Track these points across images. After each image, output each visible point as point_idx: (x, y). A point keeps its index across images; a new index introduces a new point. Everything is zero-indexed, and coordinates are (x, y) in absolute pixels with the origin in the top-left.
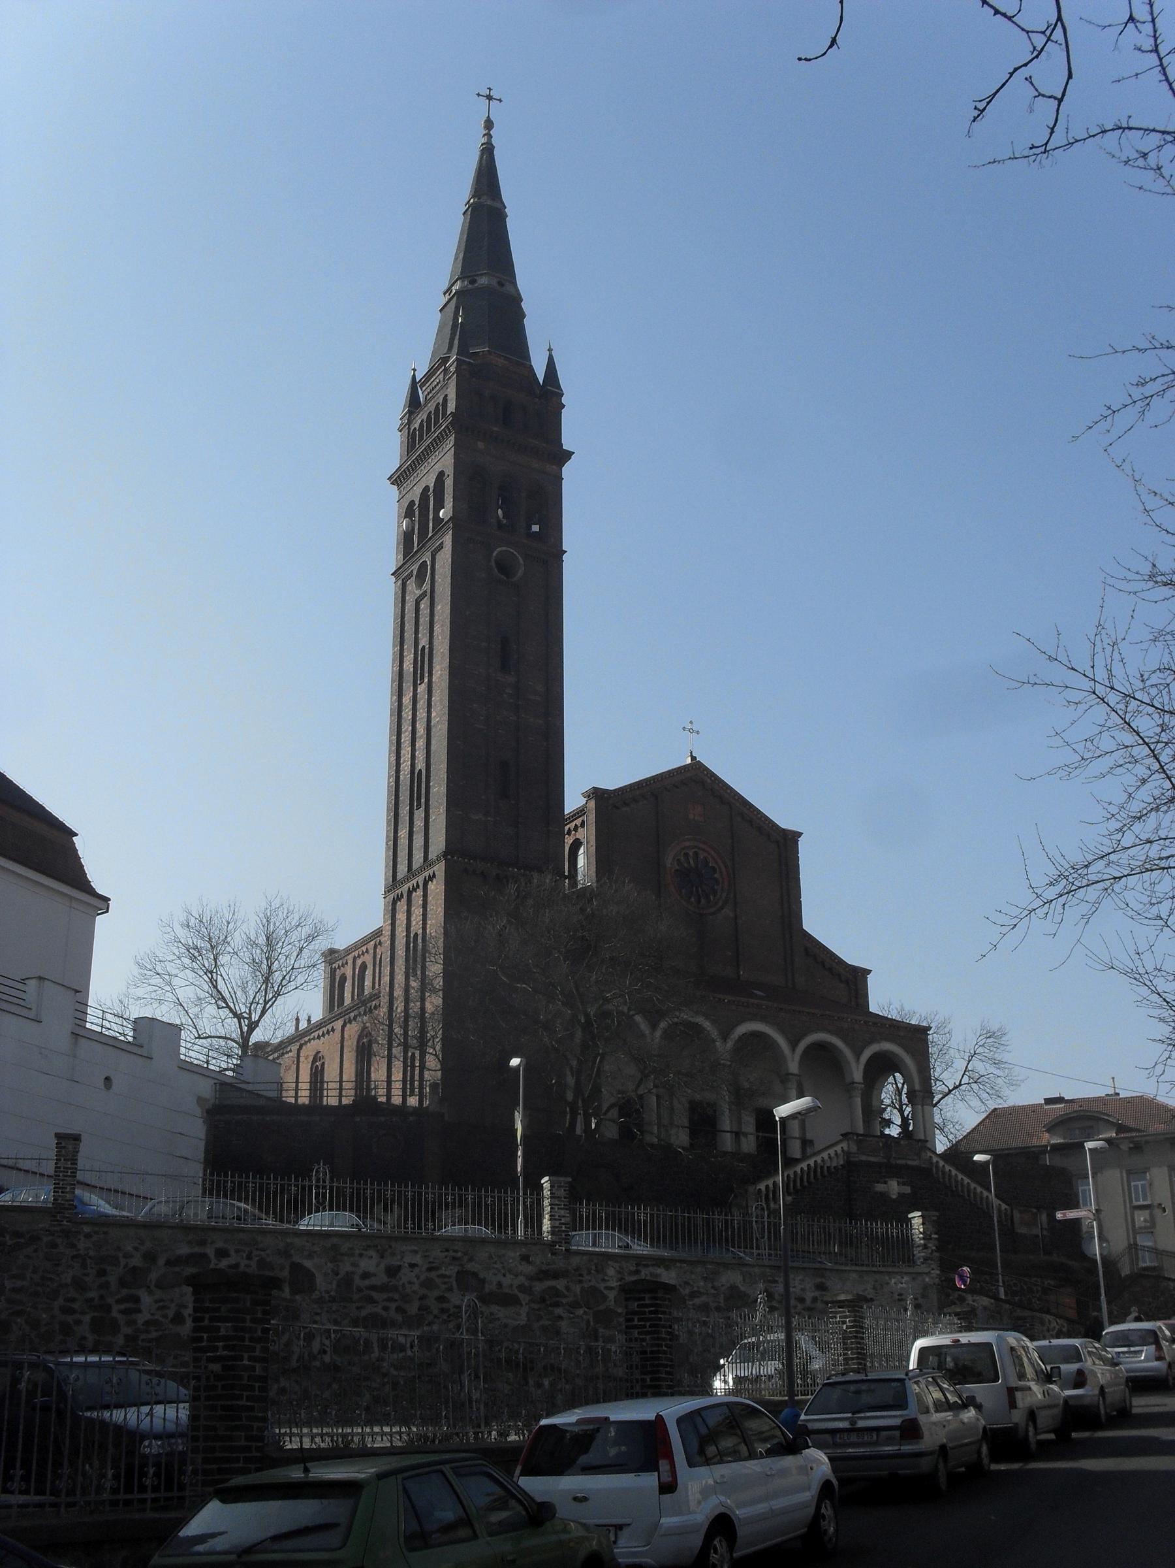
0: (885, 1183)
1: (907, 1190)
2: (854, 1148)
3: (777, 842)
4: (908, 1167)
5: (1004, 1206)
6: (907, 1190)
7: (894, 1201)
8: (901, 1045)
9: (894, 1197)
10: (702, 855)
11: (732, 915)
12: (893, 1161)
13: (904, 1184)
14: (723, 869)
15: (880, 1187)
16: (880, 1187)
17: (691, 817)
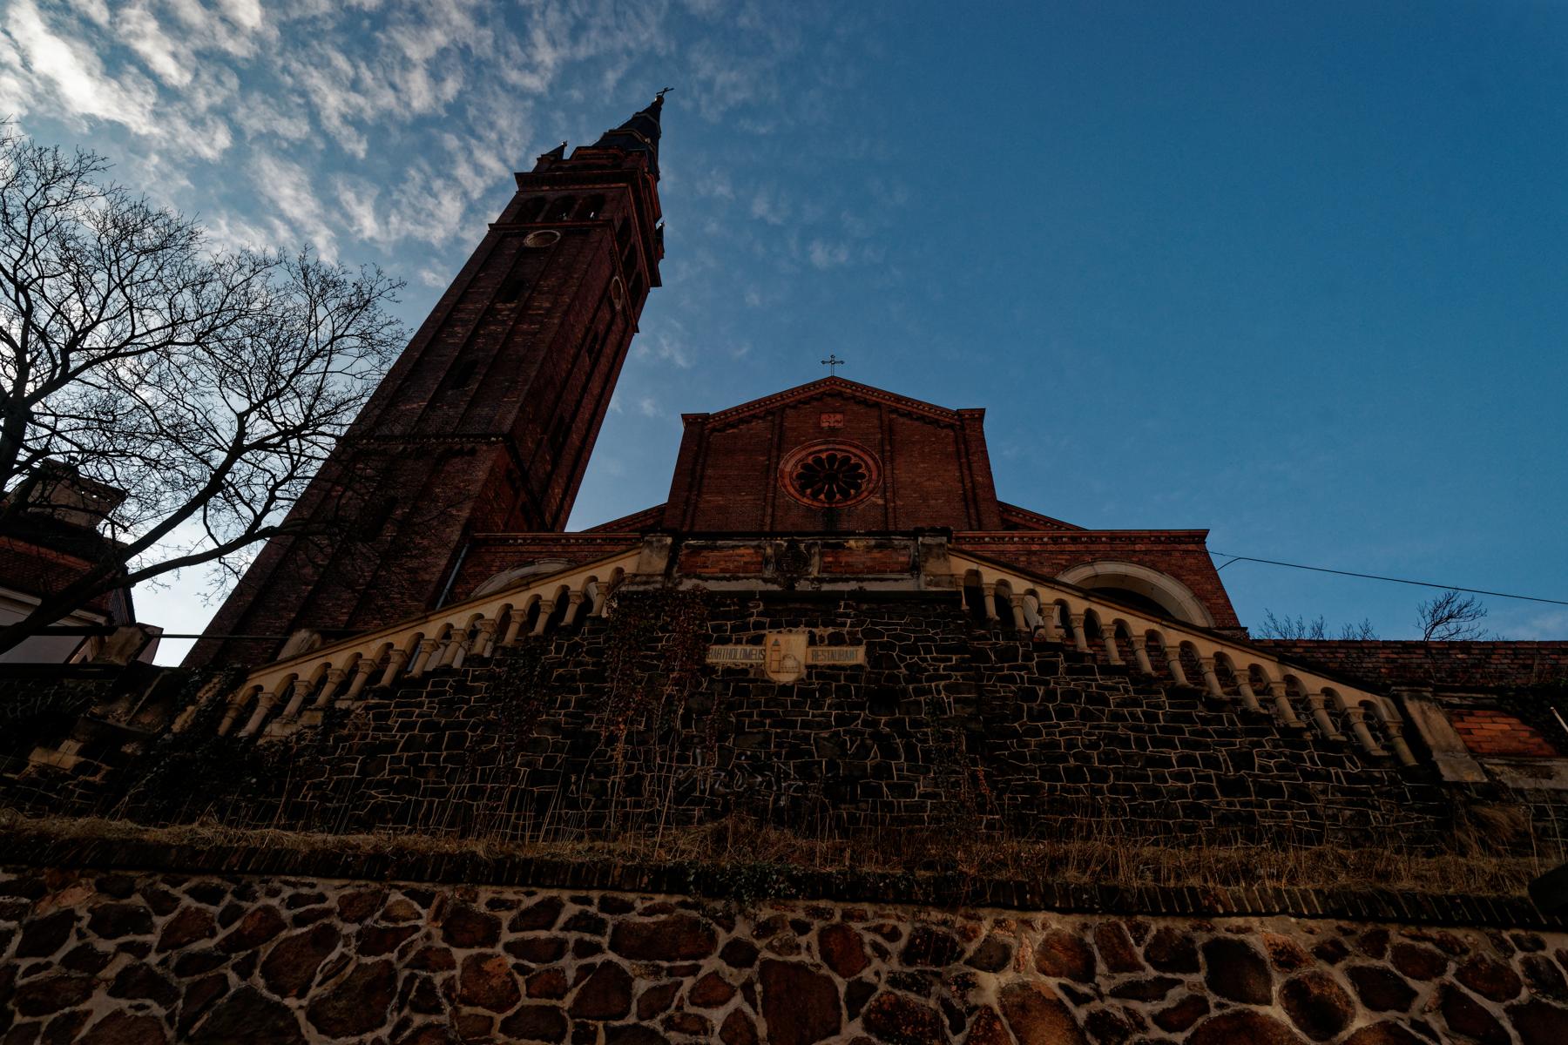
0: (758, 640)
1: (857, 655)
2: (659, 563)
3: (950, 426)
4: (859, 596)
5: (1350, 697)
6: (857, 655)
7: (786, 690)
8: (1141, 563)
9: (787, 678)
10: (839, 455)
11: (881, 502)
12: (802, 586)
13: (836, 640)
14: (871, 462)
15: (724, 656)
16: (724, 656)
17: (825, 425)
